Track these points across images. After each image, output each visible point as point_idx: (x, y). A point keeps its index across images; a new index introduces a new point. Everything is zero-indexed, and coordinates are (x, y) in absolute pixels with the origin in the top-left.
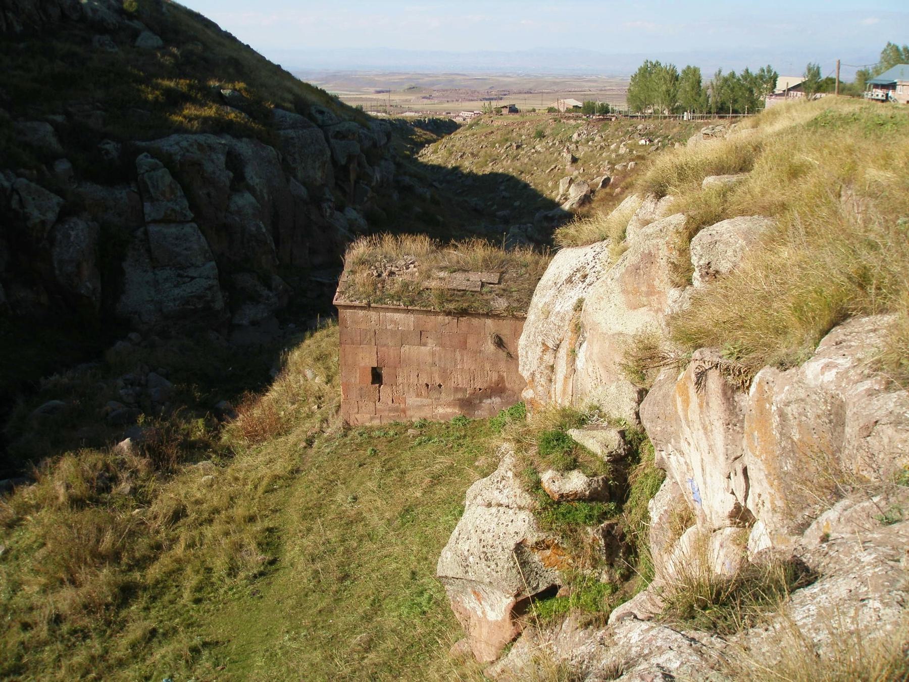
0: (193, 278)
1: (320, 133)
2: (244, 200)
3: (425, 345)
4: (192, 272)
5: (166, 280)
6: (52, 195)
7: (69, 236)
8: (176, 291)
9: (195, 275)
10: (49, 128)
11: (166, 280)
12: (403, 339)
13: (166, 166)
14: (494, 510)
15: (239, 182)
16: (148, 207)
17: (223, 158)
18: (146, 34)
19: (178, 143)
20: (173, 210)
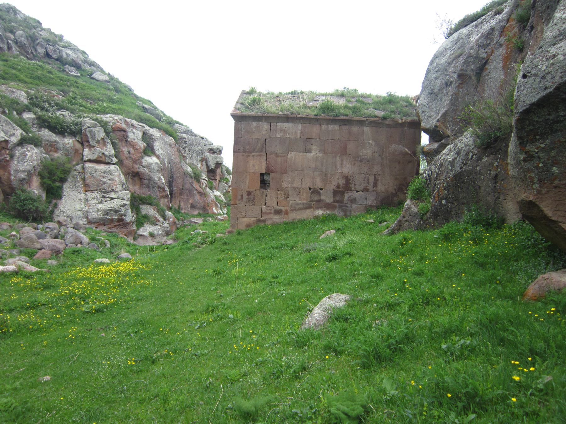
0: (112, 199)
2: (152, 160)
3: (309, 151)
4: (112, 195)
5: (94, 198)
6: (18, 128)
7: (26, 155)
9: (114, 197)
11: (94, 198)
15: (149, 150)
16: (86, 151)
17: (140, 134)
20: (103, 154)
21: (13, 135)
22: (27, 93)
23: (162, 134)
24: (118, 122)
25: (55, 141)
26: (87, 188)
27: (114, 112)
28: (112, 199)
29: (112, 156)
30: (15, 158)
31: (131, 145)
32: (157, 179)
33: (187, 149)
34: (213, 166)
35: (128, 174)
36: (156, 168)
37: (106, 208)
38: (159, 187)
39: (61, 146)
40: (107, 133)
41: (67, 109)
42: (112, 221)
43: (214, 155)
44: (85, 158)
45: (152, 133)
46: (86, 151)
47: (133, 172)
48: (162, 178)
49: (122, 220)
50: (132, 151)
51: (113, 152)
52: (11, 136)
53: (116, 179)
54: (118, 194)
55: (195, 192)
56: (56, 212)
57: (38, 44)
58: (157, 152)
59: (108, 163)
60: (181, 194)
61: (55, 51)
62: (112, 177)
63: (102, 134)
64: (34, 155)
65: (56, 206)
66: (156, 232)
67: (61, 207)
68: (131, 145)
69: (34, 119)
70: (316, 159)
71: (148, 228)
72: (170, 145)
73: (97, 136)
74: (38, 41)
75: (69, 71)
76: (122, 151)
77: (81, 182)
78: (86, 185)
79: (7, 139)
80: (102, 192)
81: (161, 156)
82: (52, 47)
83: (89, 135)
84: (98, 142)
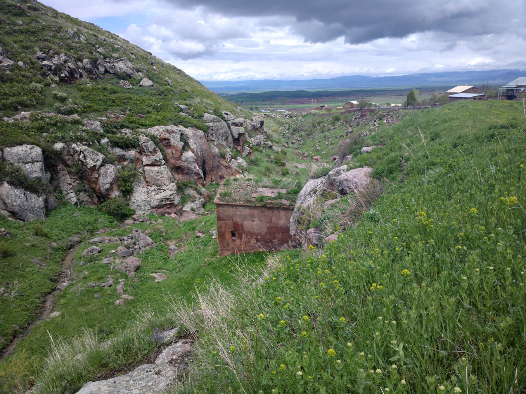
0: (165, 190)
2: (189, 154)
3: (254, 221)
4: (164, 188)
5: (153, 191)
6: (100, 153)
8: (157, 196)
10: (99, 123)
11: (153, 191)
12: (244, 217)
13: (152, 140)
15: (186, 146)
16: (144, 159)
18: (145, 79)
19: (158, 130)
20: (155, 160)
22: (101, 121)
23: (195, 130)
24: (162, 133)
25: (123, 155)
26: (148, 184)
27: (160, 123)
28: (165, 190)
29: (161, 160)
30: (101, 175)
33: (214, 135)
34: (236, 136)
35: (174, 168)
36: (192, 160)
37: (161, 197)
38: (195, 173)
39: (127, 157)
40: (156, 144)
41: (128, 127)
42: (166, 205)
43: (237, 127)
44: (144, 164)
45: (188, 133)
46: (144, 159)
47: (176, 167)
48: (197, 166)
49: (172, 204)
50: (174, 151)
51: (161, 157)
52: (97, 161)
53: (166, 176)
54: (168, 187)
55: (222, 167)
56: (130, 203)
57: (99, 64)
58: (192, 147)
59: (159, 165)
60: (212, 171)
61: (111, 67)
62: (163, 175)
63: (154, 146)
64: (112, 171)
65: (130, 199)
66: (195, 207)
67: (133, 199)
69: (108, 142)
70: (257, 225)
71: (190, 205)
72: (201, 138)
73: (150, 148)
74: (98, 62)
75: (124, 85)
76: (168, 154)
77: (143, 180)
78: (147, 182)
79: (95, 164)
80: (157, 186)
81: (195, 149)
82: (109, 64)
83: (144, 148)
84: (151, 152)
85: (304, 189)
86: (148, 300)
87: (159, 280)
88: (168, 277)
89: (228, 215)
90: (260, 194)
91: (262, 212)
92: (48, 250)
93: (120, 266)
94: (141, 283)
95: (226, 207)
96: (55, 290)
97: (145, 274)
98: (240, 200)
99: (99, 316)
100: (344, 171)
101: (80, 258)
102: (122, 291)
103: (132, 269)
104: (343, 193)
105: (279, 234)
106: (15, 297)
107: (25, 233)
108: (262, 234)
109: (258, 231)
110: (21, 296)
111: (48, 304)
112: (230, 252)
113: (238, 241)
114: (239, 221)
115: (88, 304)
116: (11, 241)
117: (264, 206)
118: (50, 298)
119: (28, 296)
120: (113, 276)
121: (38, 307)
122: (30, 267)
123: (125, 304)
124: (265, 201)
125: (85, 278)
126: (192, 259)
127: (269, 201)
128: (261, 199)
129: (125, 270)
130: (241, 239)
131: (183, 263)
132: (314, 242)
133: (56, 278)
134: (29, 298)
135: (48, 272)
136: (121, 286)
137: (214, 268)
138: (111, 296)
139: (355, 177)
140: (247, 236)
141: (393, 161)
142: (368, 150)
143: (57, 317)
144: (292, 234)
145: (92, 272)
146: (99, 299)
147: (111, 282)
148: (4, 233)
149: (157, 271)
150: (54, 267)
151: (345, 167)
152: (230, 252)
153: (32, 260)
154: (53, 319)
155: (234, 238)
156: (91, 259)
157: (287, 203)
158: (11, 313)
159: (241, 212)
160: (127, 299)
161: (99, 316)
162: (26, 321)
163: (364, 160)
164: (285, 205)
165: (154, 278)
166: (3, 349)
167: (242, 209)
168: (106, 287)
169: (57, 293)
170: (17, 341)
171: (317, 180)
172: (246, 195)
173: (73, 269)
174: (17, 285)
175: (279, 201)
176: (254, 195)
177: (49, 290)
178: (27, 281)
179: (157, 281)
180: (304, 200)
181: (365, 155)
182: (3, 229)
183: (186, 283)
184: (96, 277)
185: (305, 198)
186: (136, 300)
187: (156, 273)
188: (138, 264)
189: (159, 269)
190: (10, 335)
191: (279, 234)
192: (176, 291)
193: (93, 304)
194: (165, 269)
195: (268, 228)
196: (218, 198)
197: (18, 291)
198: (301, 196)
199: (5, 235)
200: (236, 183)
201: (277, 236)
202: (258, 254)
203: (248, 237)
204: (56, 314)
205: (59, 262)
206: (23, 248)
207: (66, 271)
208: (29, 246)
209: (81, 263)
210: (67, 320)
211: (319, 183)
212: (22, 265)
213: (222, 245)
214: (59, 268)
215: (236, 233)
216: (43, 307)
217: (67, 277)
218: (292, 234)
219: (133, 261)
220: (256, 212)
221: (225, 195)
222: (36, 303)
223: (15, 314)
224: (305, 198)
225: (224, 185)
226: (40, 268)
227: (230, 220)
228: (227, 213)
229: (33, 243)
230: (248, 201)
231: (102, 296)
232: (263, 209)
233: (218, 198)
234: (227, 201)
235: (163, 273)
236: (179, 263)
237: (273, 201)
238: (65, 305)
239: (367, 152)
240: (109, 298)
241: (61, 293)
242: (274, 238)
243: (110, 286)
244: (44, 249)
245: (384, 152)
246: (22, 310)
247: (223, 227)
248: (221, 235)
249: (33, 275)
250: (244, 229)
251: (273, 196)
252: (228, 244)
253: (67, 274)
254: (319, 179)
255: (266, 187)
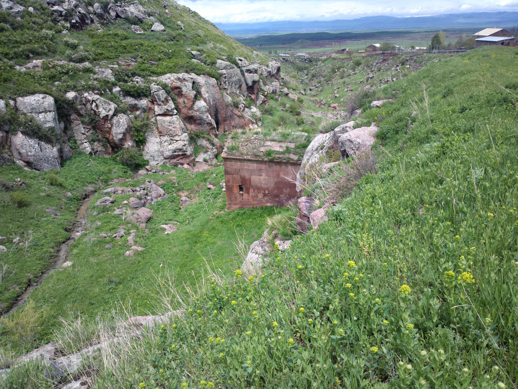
0: (177, 141)
1: (238, 71)
2: (201, 104)
3: (261, 176)
4: (177, 138)
5: (165, 141)
6: (112, 103)
7: (120, 122)
8: (170, 147)
9: (178, 139)
10: (110, 71)
11: (165, 141)
12: (252, 172)
13: (164, 89)
14: (257, 256)
15: (198, 95)
16: (156, 108)
17: (191, 85)
18: (156, 24)
19: (169, 78)
20: (167, 110)
21: (110, 109)
22: (112, 69)
23: (207, 78)
24: (174, 82)
25: (136, 104)
26: (161, 134)
28: (177, 141)
29: (173, 109)
30: (114, 125)
31: (186, 97)
32: (205, 118)
33: (227, 83)
34: (250, 84)
35: (186, 118)
36: (204, 110)
37: (174, 148)
38: (208, 123)
39: (140, 106)
40: (168, 93)
41: (139, 76)
42: (178, 156)
43: (251, 74)
44: (156, 113)
45: (200, 81)
46: (156, 108)
47: (189, 116)
48: (209, 116)
49: (185, 154)
50: (186, 100)
52: (109, 111)
53: (178, 126)
54: (180, 137)
55: (235, 116)
56: (144, 153)
57: (110, 8)
58: (204, 96)
59: (171, 115)
60: (225, 121)
61: (122, 12)
62: (175, 125)
63: (165, 95)
64: (125, 121)
65: (143, 150)
66: (208, 158)
67: (146, 149)
68: (186, 97)
69: (120, 91)
70: (265, 180)
72: (213, 86)
73: (161, 98)
74: (109, 6)
75: (135, 30)
76: (180, 103)
77: (156, 130)
78: (160, 132)
79: (107, 114)
80: (170, 136)
81: (207, 98)
82: (120, 9)
83: (156, 97)
84: (163, 102)
85: (312, 144)
86: (157, 252)
87: (169, 232)
88: (178, 229)
89: (236, 169)
90: (268, 149)
91: (270, 166)
92: (63, 199)
93: (131, 217)
94: (151, 234)
95: (234, 161)
96: (69, 239)
97: (156, 225)
98: (247, 154)
99: (110, 267)
100: (350, 128)
101: (94, 208)
102: (132, 242)
103: (144, 220)
104: (345, 154)
105: (286, 189)
106: (30, 247)
107: (40, 183)
108: (270, 189)
109: (266, 186)
110: (35, 245)
111: (62, 254)
112: (238, 206)
113: (245, 196)
114: (247, 175)
115: (99, 255)
116: (26, 191)
117: (272, 161)
118: (64, 247)
119: (43, 245)
120: (124, 227)
121: (52, 256)
122: (44, 217)
123: (134, 255)
124: (273, 155)
125: (97, 229)
126: (202, 212)
127: (277, 156)
128: (269, 154)
129: (136, 221)
130: (248, 193)
131: (193, 216)
132: (304, 212)
133: (71, 227)
134: (44, 247)
135: (62, 222)
136: (132, 237)
137: (222, 222)
138: (122, 247)
139: (358, 137)
140: (254, 190)
141: (401, 120)
142: (379, 105)
143: (68, 267)
144: (298, 191)
145: (105, 222)
146: (110, 249)
147: (122, 232)
148: (20, 183)
149: (167, 222)
150: (68, 217)
151: (351, 123)
152: (238, 206)
153: (47, 210)
154: (65, 269)
155: (241, 192)
156: (105, 209)
157: (295, 158)
158: (26, 262)
159: (249, 166)
160: (137, 251)
161: (110, 267)
162: (40, 270)
163: (372, 116)
164: (293, 160)
165: (165, 230)
166: (18, 296)
167: (249, 164)
168: (118, 238)
169: (71, 242)
170: (31, 290)
171: (325, 135)
172: (254, 148)
173: (87, 219)
174: (32, 235)
175: (287, 155)
176: (262, 149)
177: (63, 240)
178: (42, 230)
179: (166, 233)
180: (310, 156)
181: (374, 110)
182: (19, 179)
183: (194, 236)
184: (108, 228)
185: (312, 154)
186: (145, 251)
187: (166, 224)
188: (149, 215)
189: (170, 220)
190: (24, 283)
191: (286, 189)
192: (184, 244)
193: (104, 255)
194: (176, 221)
195: (276, 183)
196: (226, 152)
197: (33, 241)
198: (308, 152)
199: (21, 185)
200: (244, 136)
201: (285, 191)
202: (265, 209)
203: (256, 191)
204: (68, 263)
205: (74, 211)
206: (38, 198)
207: (80, 220)
208: (44, 196)
209: (95, 214)
210: (78, 271)
211: (327, 138)
212: (37, 215)
213: (230, 199)
214: (74, 217)
215: (244, 187)
216: (57, 256)
217: (81, 226)
218: (298, 191)
219: (144, 212)
220: (263, 167)
221: (233, 148)
222: (50, 252)
223: (29, 263)
224: (312, 154)
225: (232, 138)
226: (54, 218)
227: (237, 174)
228: (235, 167)
229: (48, 193)
230: (256, 156)
231: (113, 247)
232: (271, 164)
233: (226, 152)
234: (234, 155)
235: (174, 224)
236: (188, 215)
237: (281, 156)
238: (77, 255)
239: (377, 106)
240: (120, 249)
241: (75, 243)
242: (282, 193)
243: (122, 237)
244: (59, 199)
245: (395, 106)
246: (37, 259)
247: (231, 181)
248: (229, 189)
249: (47, 224)
250: (252, 184)
251: (281, 150)
252: (236, 198)
253: (81, 224)
254: (328, 134)
255: (274, 141)
